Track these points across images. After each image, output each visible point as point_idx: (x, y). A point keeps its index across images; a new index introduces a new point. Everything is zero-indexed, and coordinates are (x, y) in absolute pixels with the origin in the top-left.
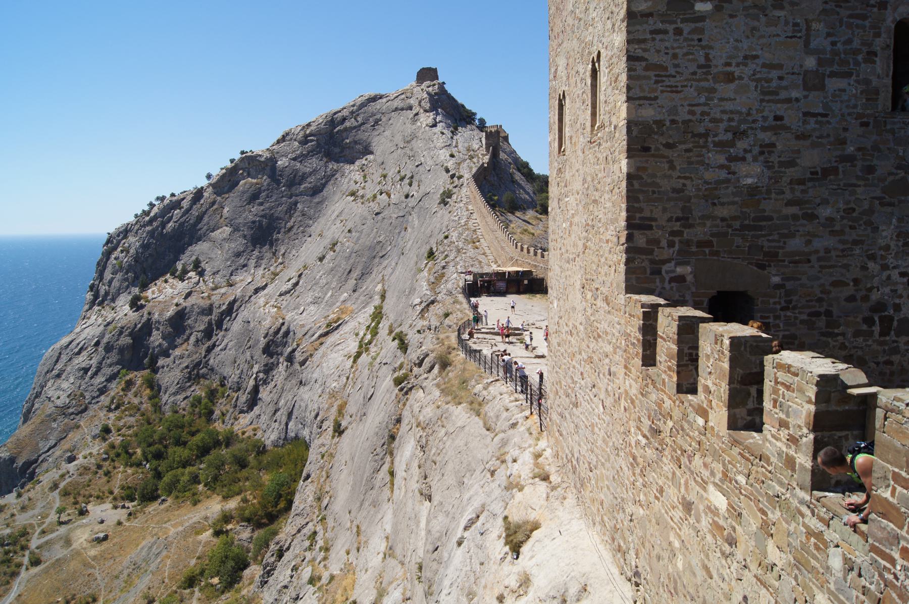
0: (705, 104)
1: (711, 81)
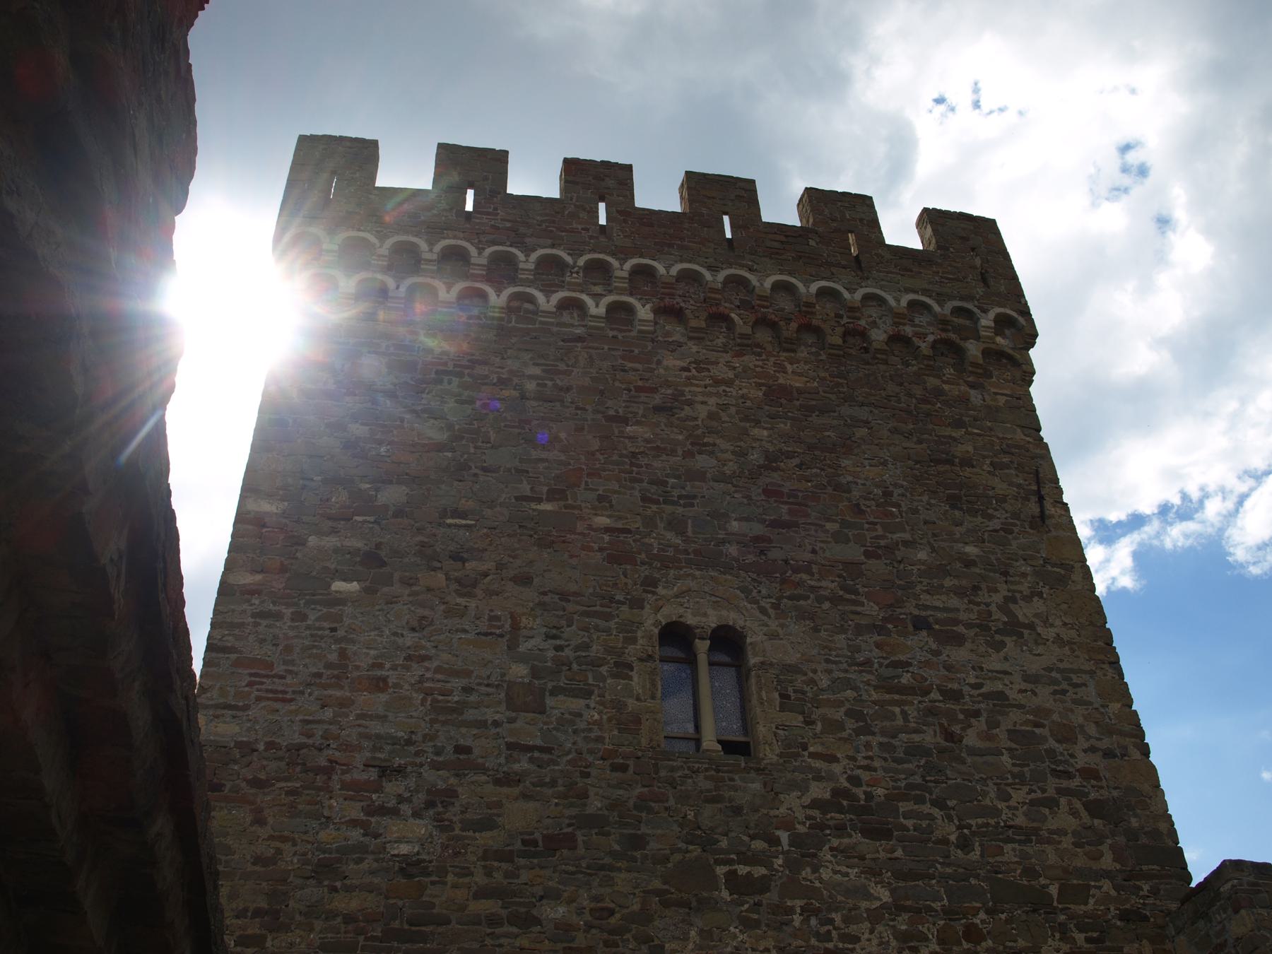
1: (347, 688)
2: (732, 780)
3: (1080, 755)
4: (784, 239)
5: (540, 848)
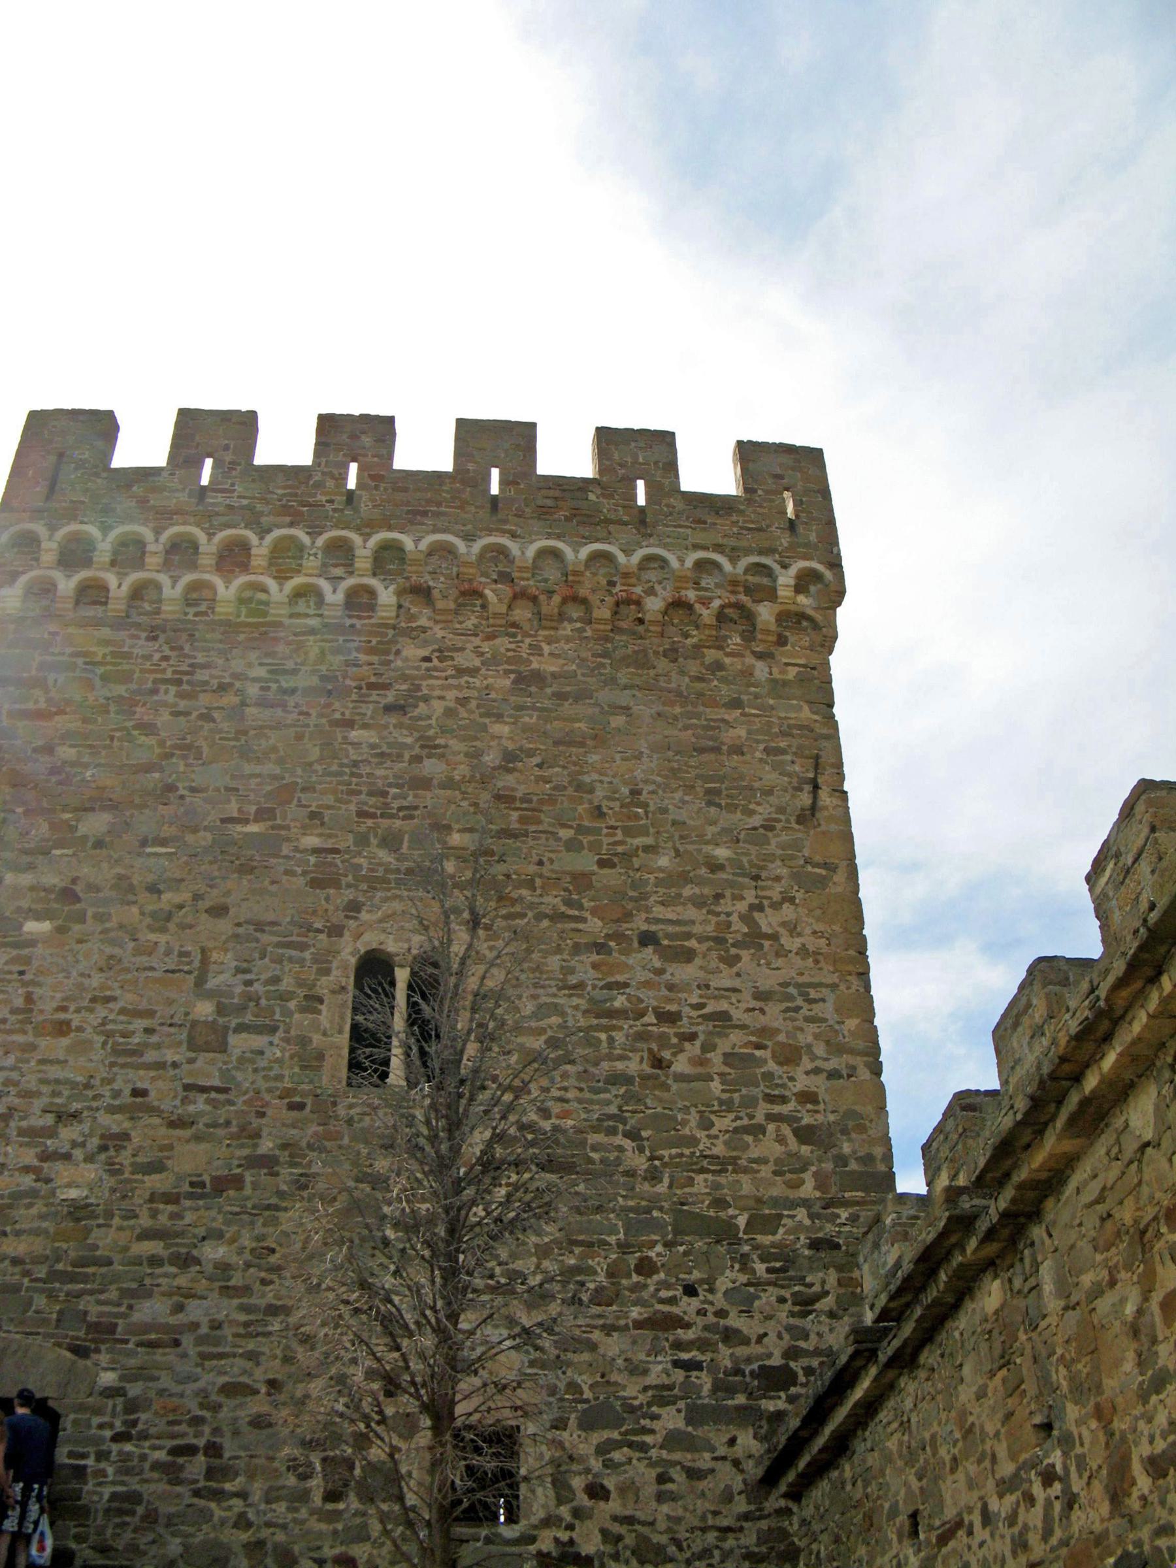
0: (12, 1069)
4: (557, 493)
5: (208, 1189)
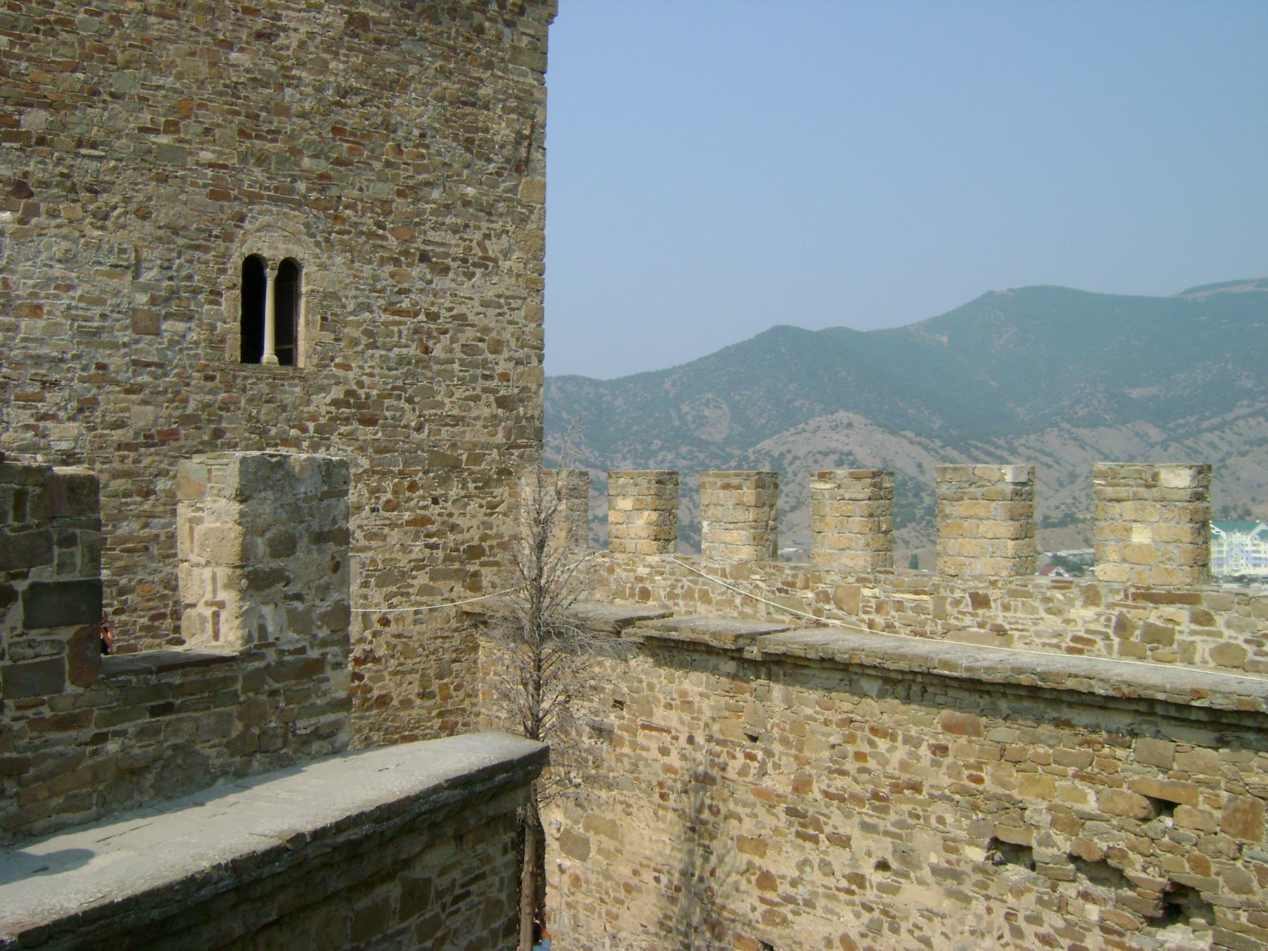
2: (283, 385)
3: (502, 363)
